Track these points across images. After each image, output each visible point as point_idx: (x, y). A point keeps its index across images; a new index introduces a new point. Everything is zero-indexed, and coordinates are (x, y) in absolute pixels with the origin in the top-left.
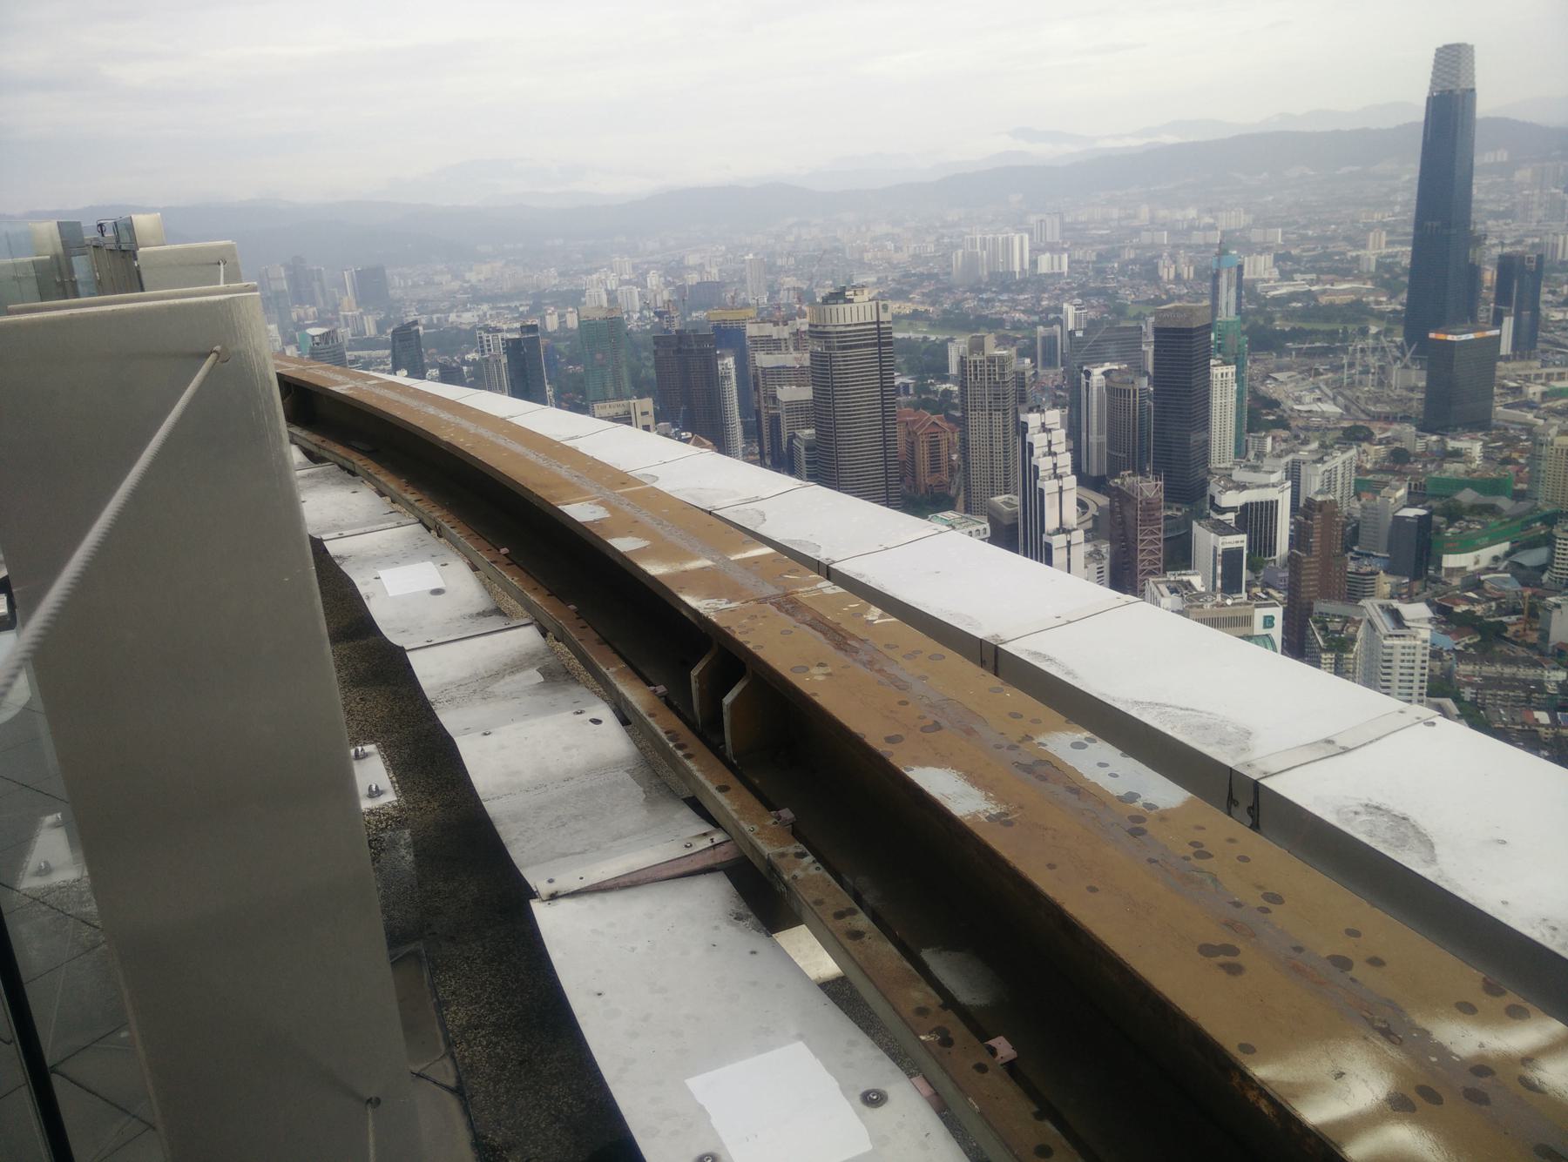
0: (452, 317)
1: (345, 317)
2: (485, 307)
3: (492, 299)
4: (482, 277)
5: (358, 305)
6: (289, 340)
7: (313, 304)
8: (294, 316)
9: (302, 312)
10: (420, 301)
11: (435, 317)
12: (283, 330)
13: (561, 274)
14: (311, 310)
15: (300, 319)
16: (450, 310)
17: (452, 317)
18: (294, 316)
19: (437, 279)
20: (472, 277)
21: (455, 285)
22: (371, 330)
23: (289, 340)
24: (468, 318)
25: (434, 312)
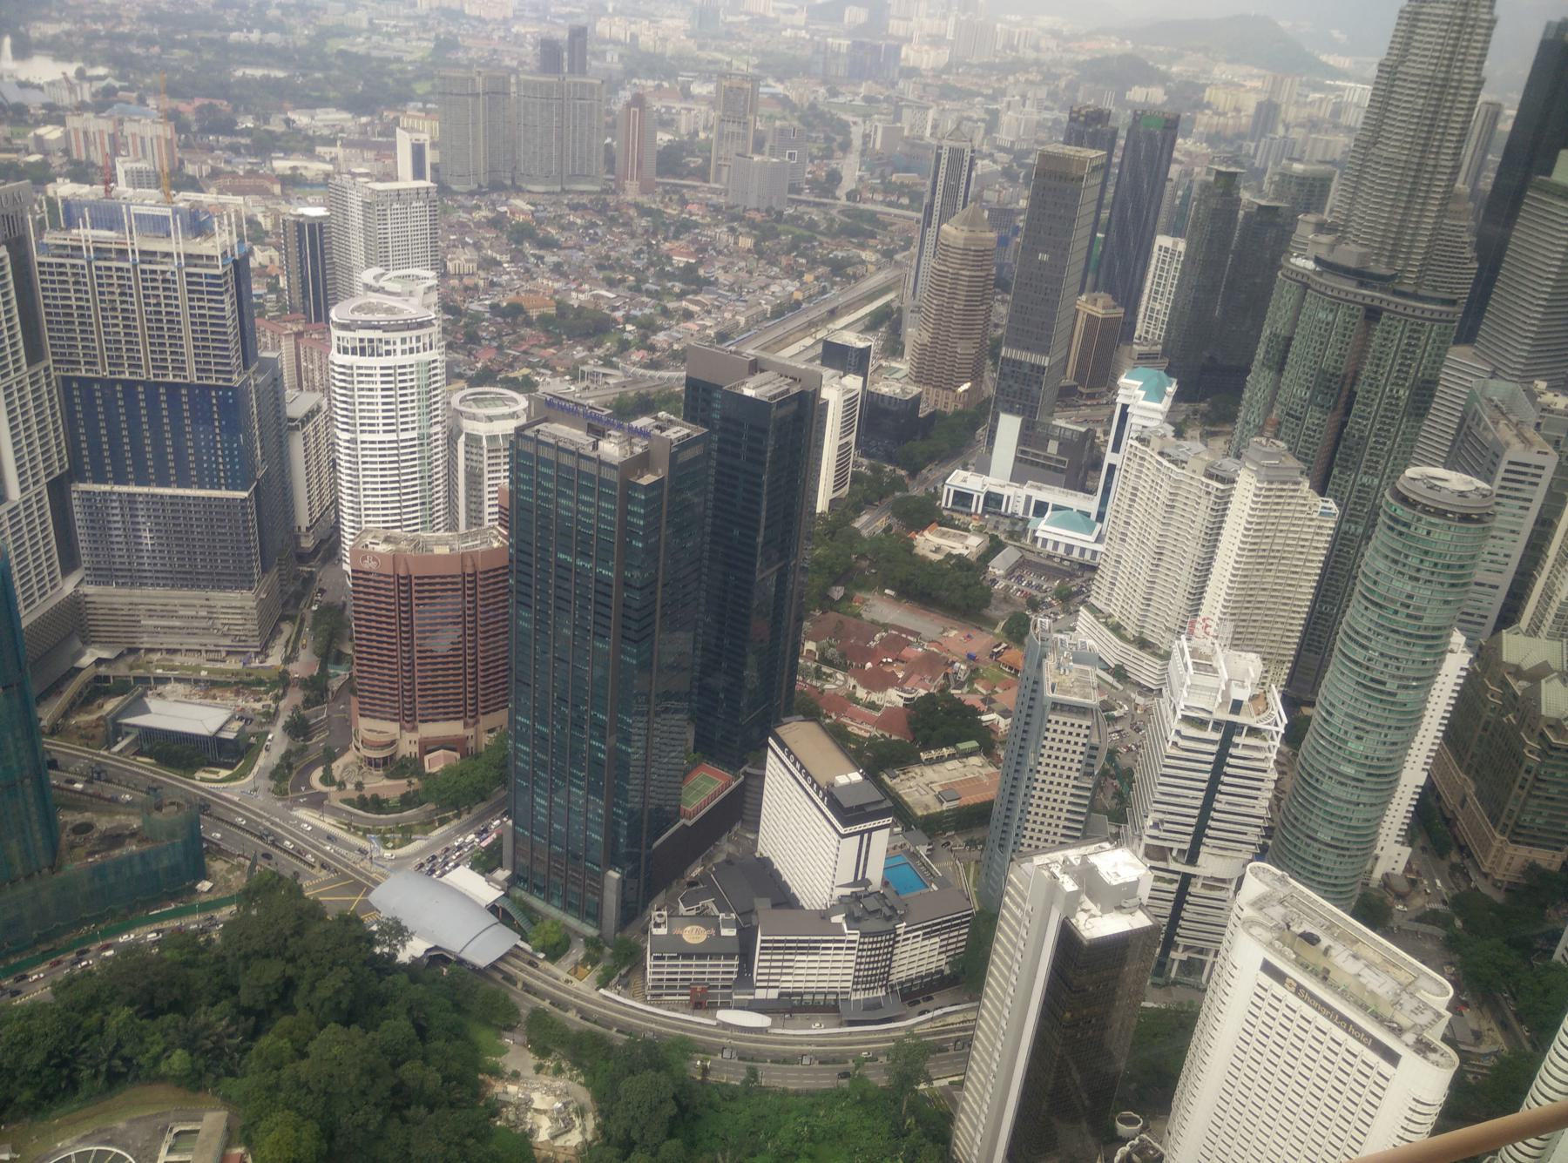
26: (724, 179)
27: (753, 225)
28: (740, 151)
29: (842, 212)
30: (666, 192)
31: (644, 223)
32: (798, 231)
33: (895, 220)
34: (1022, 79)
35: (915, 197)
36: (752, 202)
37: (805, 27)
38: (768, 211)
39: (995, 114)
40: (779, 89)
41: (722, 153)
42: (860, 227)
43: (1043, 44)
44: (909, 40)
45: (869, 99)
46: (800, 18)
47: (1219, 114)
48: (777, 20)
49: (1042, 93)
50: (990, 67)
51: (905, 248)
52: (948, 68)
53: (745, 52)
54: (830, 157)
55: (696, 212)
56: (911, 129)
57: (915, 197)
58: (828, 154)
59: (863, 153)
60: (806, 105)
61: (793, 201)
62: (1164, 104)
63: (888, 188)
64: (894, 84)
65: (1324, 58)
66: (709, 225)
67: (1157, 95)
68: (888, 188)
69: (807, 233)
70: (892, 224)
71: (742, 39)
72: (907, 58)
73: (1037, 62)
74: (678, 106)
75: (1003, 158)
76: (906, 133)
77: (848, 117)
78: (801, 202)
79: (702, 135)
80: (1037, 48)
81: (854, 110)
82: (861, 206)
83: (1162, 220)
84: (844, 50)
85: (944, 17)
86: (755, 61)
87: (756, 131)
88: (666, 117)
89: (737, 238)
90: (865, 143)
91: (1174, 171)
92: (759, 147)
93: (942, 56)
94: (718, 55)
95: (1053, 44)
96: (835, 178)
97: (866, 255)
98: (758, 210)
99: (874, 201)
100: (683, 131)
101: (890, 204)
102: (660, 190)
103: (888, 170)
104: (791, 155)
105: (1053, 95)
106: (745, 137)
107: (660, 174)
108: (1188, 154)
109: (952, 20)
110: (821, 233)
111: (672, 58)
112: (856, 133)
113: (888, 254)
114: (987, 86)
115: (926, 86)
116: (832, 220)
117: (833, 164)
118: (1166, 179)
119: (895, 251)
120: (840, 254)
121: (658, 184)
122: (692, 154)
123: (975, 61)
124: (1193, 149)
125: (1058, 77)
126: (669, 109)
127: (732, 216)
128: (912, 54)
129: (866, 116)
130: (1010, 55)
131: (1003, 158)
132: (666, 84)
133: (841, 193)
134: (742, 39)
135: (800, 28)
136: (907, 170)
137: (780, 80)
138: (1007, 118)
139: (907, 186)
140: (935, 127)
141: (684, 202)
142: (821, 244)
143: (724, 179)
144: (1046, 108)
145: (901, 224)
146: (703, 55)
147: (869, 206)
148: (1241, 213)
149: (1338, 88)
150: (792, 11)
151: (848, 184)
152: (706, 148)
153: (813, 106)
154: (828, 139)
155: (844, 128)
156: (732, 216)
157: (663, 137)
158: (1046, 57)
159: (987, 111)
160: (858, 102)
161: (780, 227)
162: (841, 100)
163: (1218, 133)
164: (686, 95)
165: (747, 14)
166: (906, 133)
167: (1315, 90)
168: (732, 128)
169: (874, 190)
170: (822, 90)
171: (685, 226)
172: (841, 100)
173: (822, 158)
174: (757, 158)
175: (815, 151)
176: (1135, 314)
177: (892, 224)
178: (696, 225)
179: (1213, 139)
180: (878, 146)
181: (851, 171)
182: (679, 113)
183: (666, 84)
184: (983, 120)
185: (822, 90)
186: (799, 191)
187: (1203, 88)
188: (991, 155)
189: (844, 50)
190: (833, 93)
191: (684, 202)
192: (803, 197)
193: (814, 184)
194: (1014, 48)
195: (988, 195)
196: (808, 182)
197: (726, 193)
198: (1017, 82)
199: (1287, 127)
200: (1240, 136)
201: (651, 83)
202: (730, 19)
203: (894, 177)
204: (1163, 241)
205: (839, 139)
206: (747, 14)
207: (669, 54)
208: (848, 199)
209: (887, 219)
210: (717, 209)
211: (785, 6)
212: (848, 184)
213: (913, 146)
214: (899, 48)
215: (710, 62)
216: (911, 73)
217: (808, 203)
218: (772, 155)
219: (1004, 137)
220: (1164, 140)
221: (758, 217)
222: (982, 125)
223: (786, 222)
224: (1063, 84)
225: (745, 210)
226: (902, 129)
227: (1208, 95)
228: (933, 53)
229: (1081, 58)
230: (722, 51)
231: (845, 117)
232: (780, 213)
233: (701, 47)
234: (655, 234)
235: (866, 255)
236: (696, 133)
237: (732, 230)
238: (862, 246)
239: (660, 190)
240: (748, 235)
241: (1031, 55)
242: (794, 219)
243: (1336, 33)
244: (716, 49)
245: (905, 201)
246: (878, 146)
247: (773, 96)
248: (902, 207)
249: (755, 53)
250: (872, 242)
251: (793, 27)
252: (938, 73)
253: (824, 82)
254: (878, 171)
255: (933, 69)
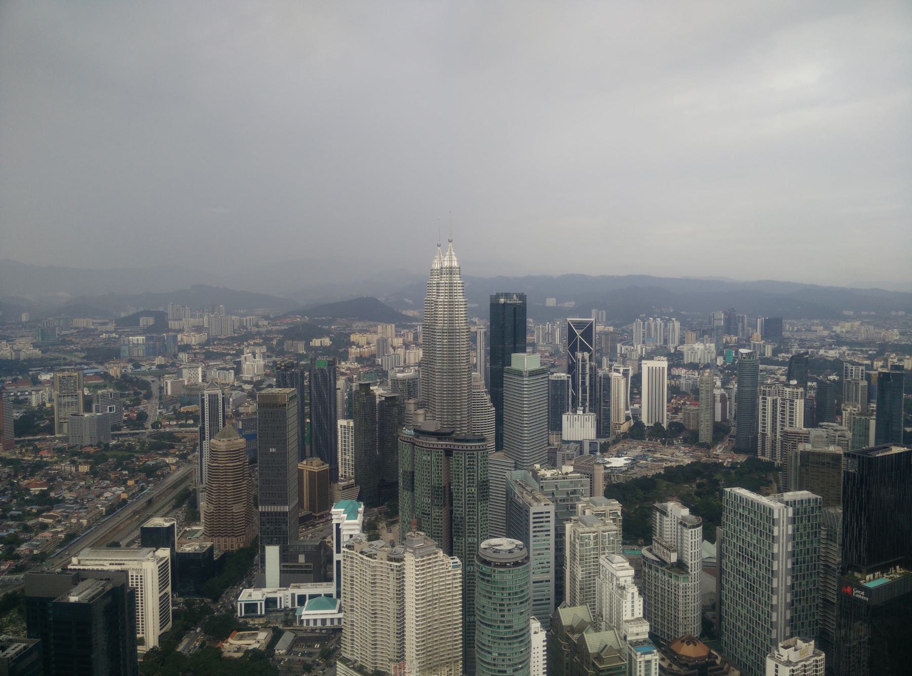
0: (822, 352)
1: (754, 345)
2: (844, 348)
3: (851, 344)
4: (844, 330)
5: (762, 338)
6: (720, 353)
7: (736, 335)
8: (724, 340)
9: (728, 338)
10: (801, 340)
11: (810, 351)
12: (717, 348)
13: (902, 334)
14: (734, 338)
15: (727, 342)
16: (820, 348)
17: (822, 352)
18: (724, 340)
19: (813, 328)
20: (837, 329)
21: (826, 333)
22: (768, 353)
23: (720, 353)
24: (832, 354)
25: (809, 348)
26: (65, 430)
27: (88, 456)
28: (75, 412)
29: (151, 436)
30: (22, 446)
31: (7, 470)
32: (120, 454)
33: (186, 435)
34: (252, 343)
35: (197, 418)
36: (87, 441)
37: (115, 332)
38: (99, 445)
39: (239, 364)
40: (101, 369)
41: (62, 415)
42: (164, 443)
43: (260, 323)
44: (181, 331)
45: (159, 366)
46: (111, 327)
47: (360, 347)
48: (94, 330)
49: (264, 349)
50: (232, 339)
51: (194, 451)
52: (208, 342)
53: (76, 350)
54: (139, 404)
55: (47, 456)
56: (189, 381)
57: (196, 420)
58: (137, 402)
59: (160, 398)
60: (119, 376)
61: (116, 435)
62: (331, 346)
63: (178, 416)
64: (175, 356)
65: (404, 312)
66: (56, 462)
67: (327, 342)
68: (178, 416)
69: (127, 454)
70: (184, 438)
71: (73, 343)
72: (182, 340)
73: (259, 333)
74: (30, 389)
75: (248, 387)
76: (186, 383)
77: (149, 379)
78: (121, 435)
79: (48, 405)
80: (257, 326)
81: (151, 373)
82: (162, 430)
83: (339, 410)
84: (140, 342)
85: (201, 316)
86: (83, 355)
87: (84, 396)
88: (21, 398)
89: (77, 467)
90: (161, 392)
91: (341, 383)
92: (88, 409)
93: (204, 337)
94: (57, 355)
95: (265, 323)
96: (143, 417)
97: (169, 460)
98: (91, 446)
99: (170, 426)
100: (34, 404)
101: (181, 426)
102: (18, 446)
103: (179, 405)
104: (110, 409)
105: (270, 349)
106: (77, 403)
107: (16, 435)
108: (349, 369)
109: (206, 318)
110: (137, 452)
111: (25, 360)
112: (155, 390)
113: (183, 457)
114: (232, 349)
115: (195, 354)
116: (144, 442)
117: (141, 407)
118: (336, 389)
119: (188, 454)
120: (151, 463)
121: (17, 442)
122: (41, 418)
123: (223, 337)
124: (351, 366)
125: (272, 339)
126: (23, 392)
127: (73, 453)
128: (185, 338)
129: (160, 377)
130: (243, 332)
131: (248, 387)
132: (20, 377)
133: (148, 425)
134: (73, 343)
135: (111, 332)
136: (189, 403)
137: (101, 364)
138: (246, 366)
139: (191, 413)
140: (204, 376)
141: (37, 451)
142: (138, 459)
143: (65, 430)
144: (268, 356)
145: (189, 436)
146: (47, 355)
147: (168, 430)
148: (378, 400)
149: (414, 326)
150: (106, 324)
151: (151, 420)
152: (51, 412)
153: (124, 376)
154: (136, 393)
155: (146, 385)
156: (73, 453)
157: (17, 414)
158: (264, 329)
159: (235, 363)
160: (154, 368)
161: (108, 454)
162: (143, 369)
163: (361, 356)
164: (36, 382)
165: (75, 328)
166: (186, 383)
167: (404, 328)
168: (67, 400)
169: (170, 419)
170: (130, 366)
171: (38, 466)
172: (143, 369)
173: (133, 406)
174: (86, 415)
175: (128, 402)
176: (337, 463)
177: (184, 438)
178: (47, 464)
179: (360, 359)
180: (169, 393)
181: (153, 410)
182: (30, 394)
183: (20, 377)
184: (232, 369)
185: (130, 366)
186: (119, 429)
187: (349, 335)
188: (240, 386)
189: (140, 342)
190: (137, 366)
191: (37, 451)
192: (123, 432)
193: (130, 423)
194: (244, 328)
195: (241, 410)
196: (125, 421)
197: (66, 439)
198: (250, 345)
199: (394, 348)
200: (373, 356)
201: (9, 378)
202: (63, 333)
203: (182, 409)
204: (341, 422)
205: (144, 392)
206: (75, 328)
207: (22, 358)
208: (153, 427)
209: (180, 435)
210: (60, 451)
211: (100, 321)
212: (153, 417)
213: (192, 389)
214: (175, 337)
215: (51, 360)
216: (186, 348)
217: (125, 435)
218: (97, 411)
219: (246, 376)
220: (330, 372)
221: (92, 450)
222: (232, 371)
223: (112, 449)
224: (275, 342)
225: (82, 447)
226: (183, 381)
227: (353, 338)
228: (197, 336)
229: (283, 328)
230: (59, 351)
231: (145, 378)
232: (107, 445)
233: (43, 352)
234: (16, 476)
235: (169, 460)
236: (44, 404)
237: (73, 463)
238: (166, 455)
239: (18, 446)
240: (85, 463)
241: (255, 330)
242: (116, 447)
243: (407, 300)
244: (55, 352)
245: (191, 422)
246: (169, 393)
247: (96, 374)
248: (190, 426)
249: (82, 350)
250: (172, 451)
251: (107, 332)
252: (202, 345)
253: (130, 361)
254: (171, 407)
255: (199, 344)
